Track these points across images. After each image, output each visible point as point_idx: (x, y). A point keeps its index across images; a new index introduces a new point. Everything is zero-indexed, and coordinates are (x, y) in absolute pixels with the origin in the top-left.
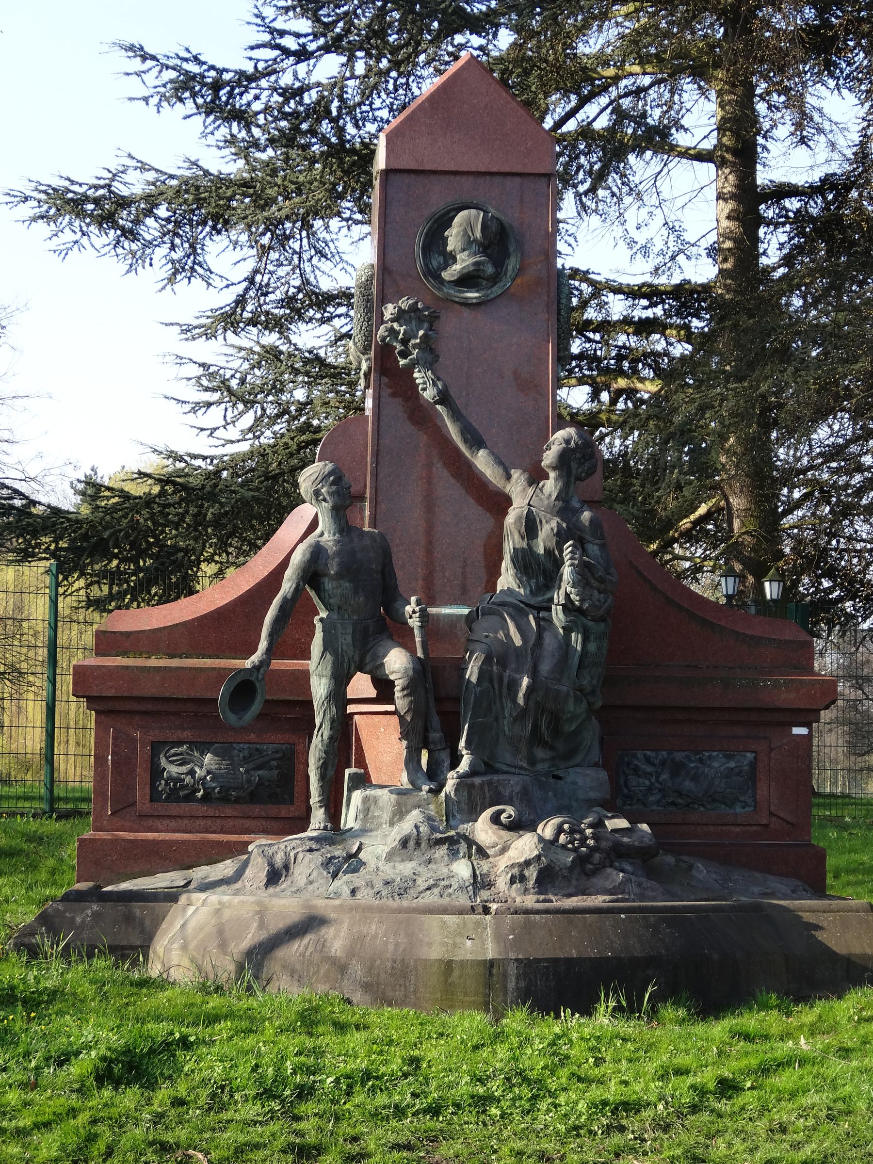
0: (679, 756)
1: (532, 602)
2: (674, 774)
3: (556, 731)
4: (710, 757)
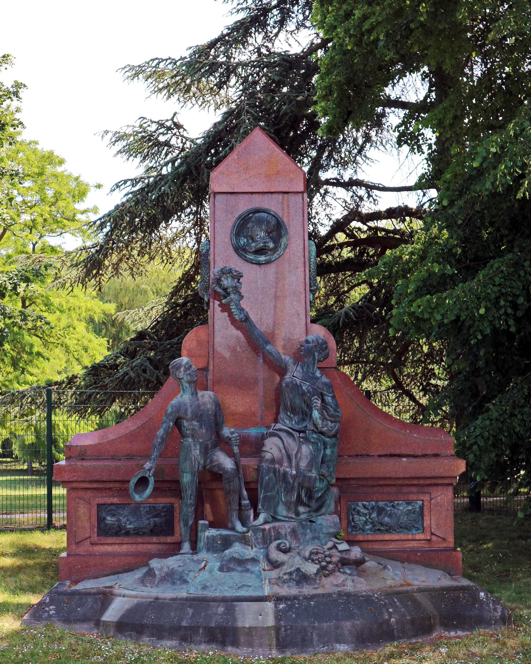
0: (381, 504)
1: (296, 427)
2: (379, 514)
3: (310, 497)
4: (398, 504)
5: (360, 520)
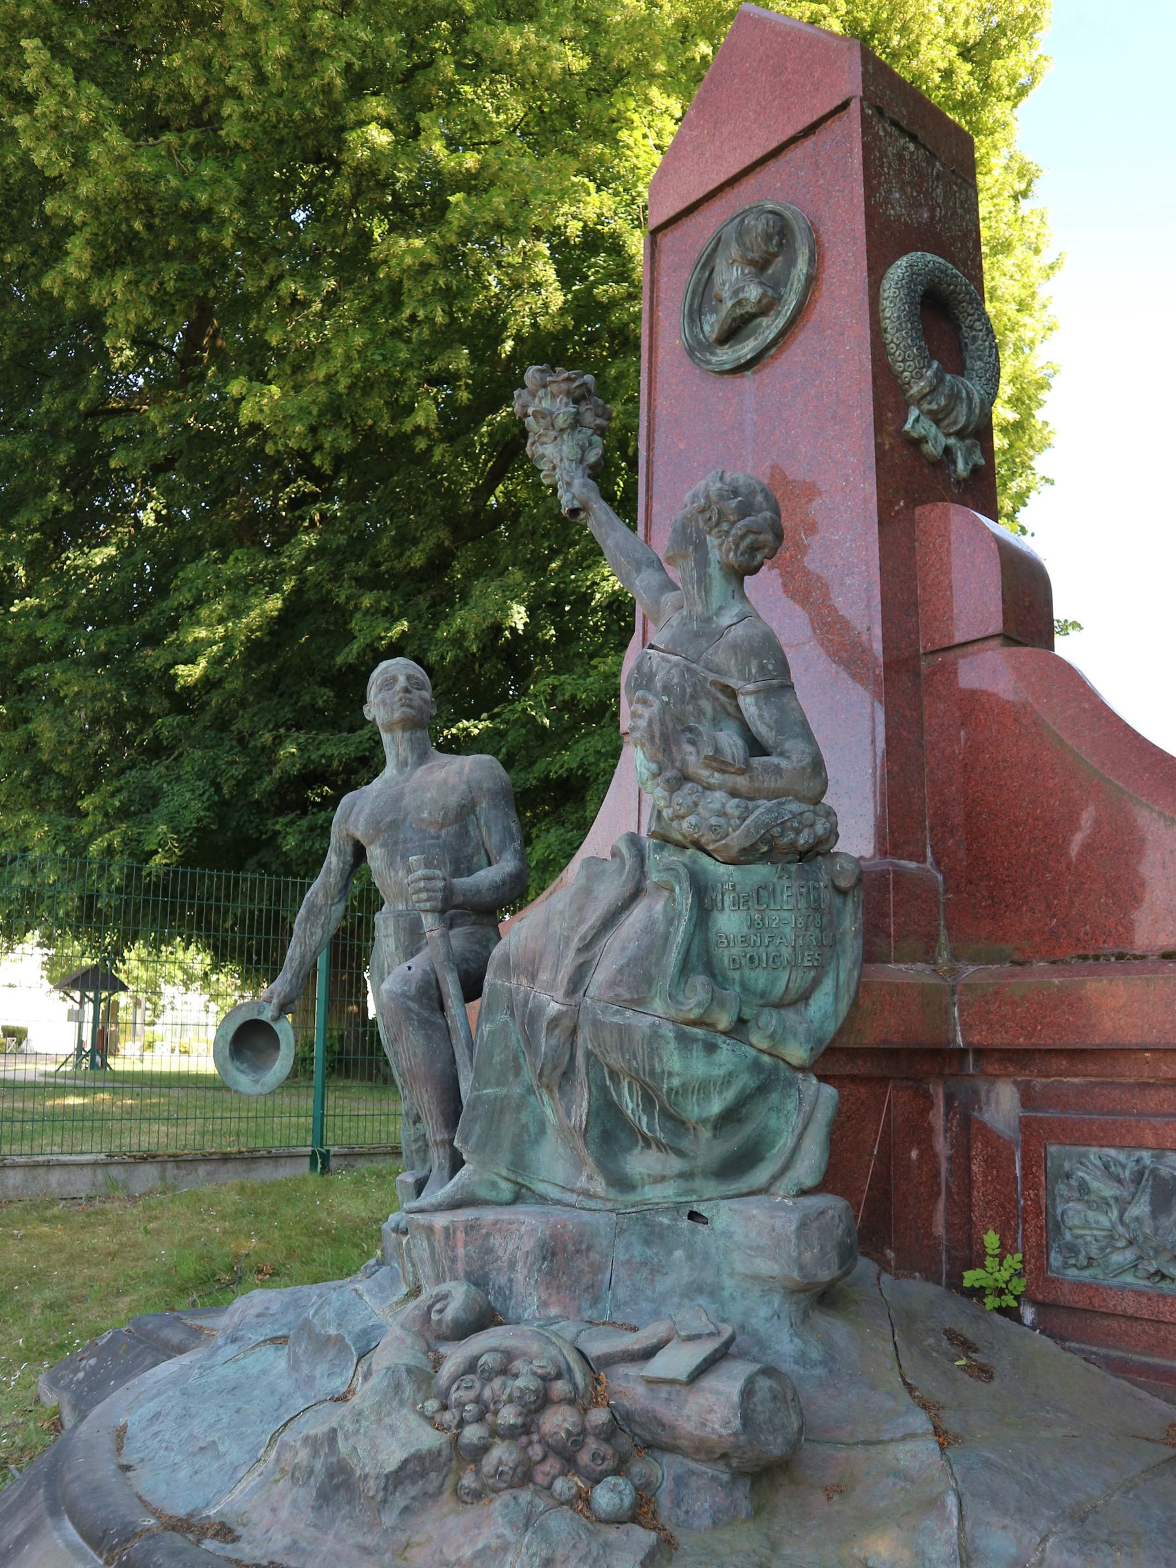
5: (1086, 1225)
